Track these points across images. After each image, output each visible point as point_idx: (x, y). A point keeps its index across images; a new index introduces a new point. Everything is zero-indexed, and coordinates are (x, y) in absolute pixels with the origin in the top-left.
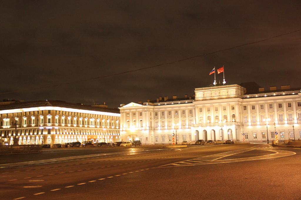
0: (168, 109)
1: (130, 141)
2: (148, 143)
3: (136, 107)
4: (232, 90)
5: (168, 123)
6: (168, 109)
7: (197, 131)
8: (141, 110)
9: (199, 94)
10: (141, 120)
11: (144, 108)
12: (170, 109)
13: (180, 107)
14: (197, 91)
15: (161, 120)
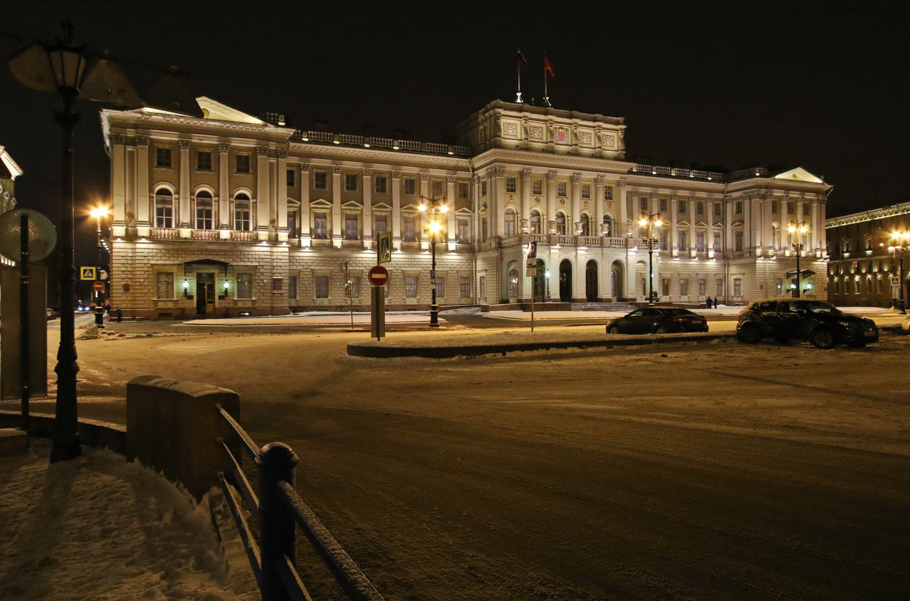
0: (347, 165)
1: (186, 290)
2: (279, 305)
3: (225, 126)
4: (610, 136)
5: (344, 225)
6: (347, 165)
7: (566, 268)
8: (251, 144)
9: (512, 126)
10: (248, 193)
11: (268, 138)
12: (356, 166)
13: (398, 164)
14: (503, 112)
15: (311, 208)
